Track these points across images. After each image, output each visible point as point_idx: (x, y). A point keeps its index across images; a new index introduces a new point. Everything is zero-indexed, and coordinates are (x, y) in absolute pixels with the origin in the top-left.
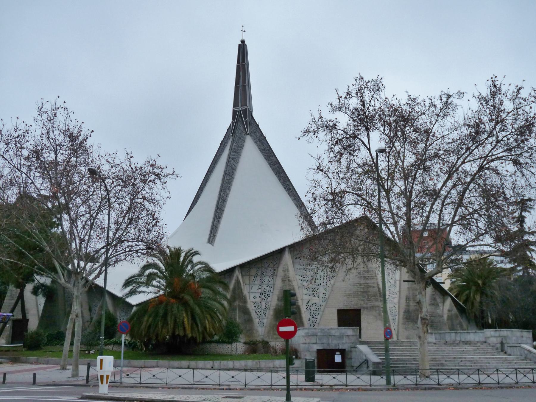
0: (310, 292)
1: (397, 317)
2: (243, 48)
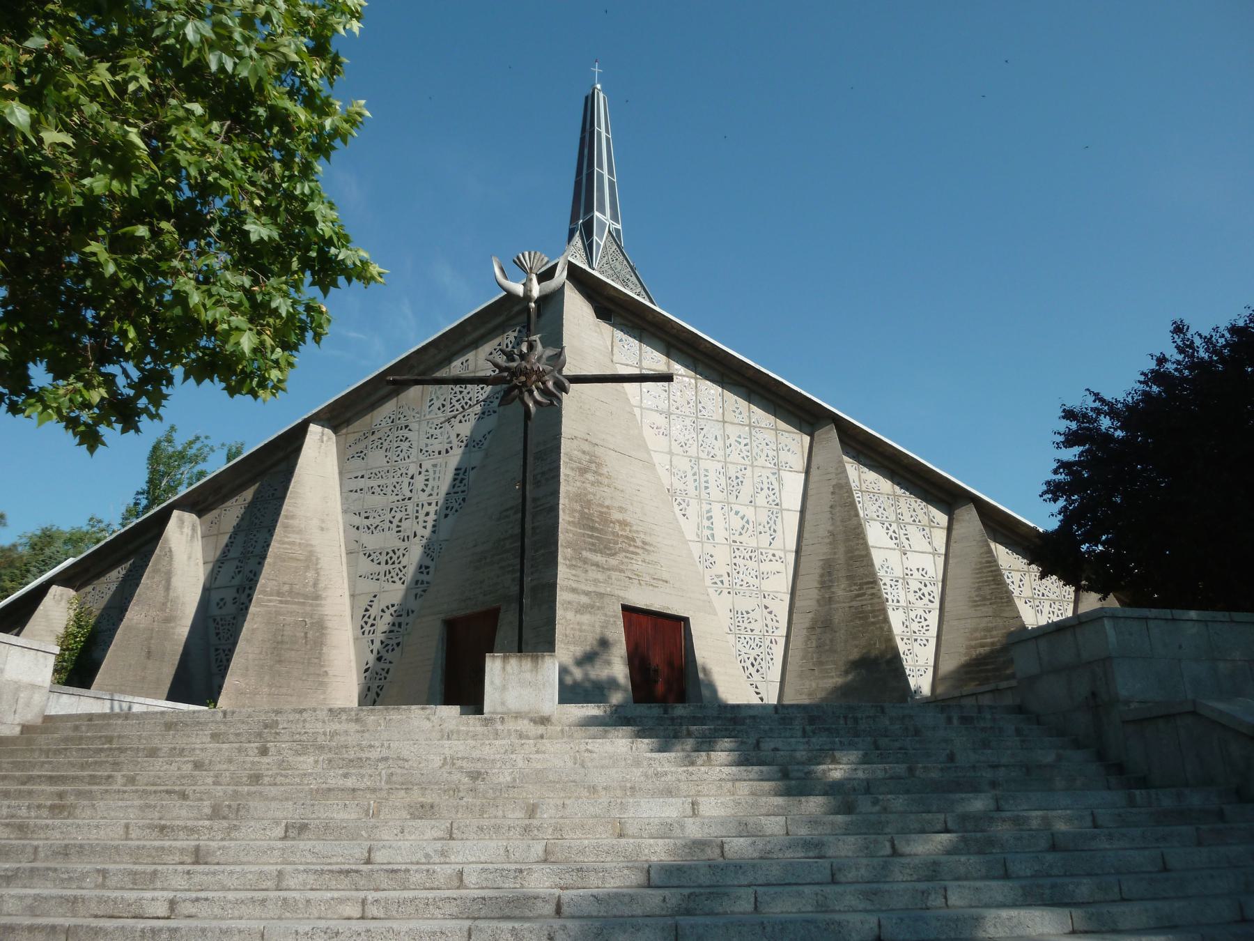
0: (377, 568)
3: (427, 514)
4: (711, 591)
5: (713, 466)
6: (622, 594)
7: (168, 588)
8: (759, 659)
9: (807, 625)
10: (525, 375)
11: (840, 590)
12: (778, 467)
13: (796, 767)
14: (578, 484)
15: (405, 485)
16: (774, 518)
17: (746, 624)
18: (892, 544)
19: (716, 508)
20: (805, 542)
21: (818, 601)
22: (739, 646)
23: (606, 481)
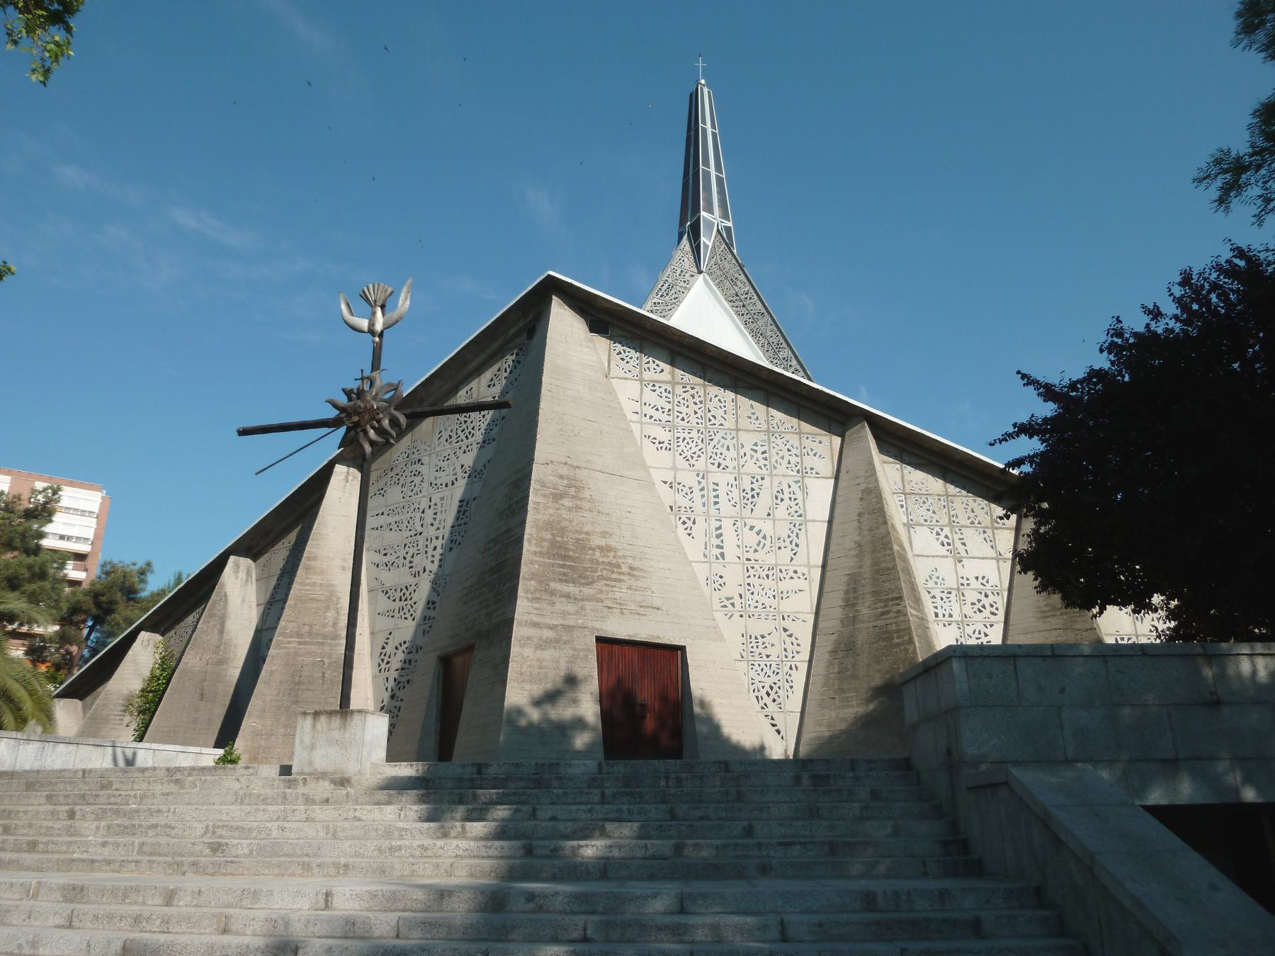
1: (799, 679)
3: (435, 548)
4: (719, 616)
5: (724, 478)
6: (597, 625)
7: (222, 632)
8: (776, 688)
9: (830, 648)
10: (358, 414)
11: (865, 610)
12: (803, 472)
13: (541, 843)
14: (551, 511)
15: (417, 520)
16: (796, 530)
17: (760, 650)
18: (943, 551)
19: (727, 525)
20: (831, 555)
21: (842, 621)
22: (752, 674)
23: (586, 505)
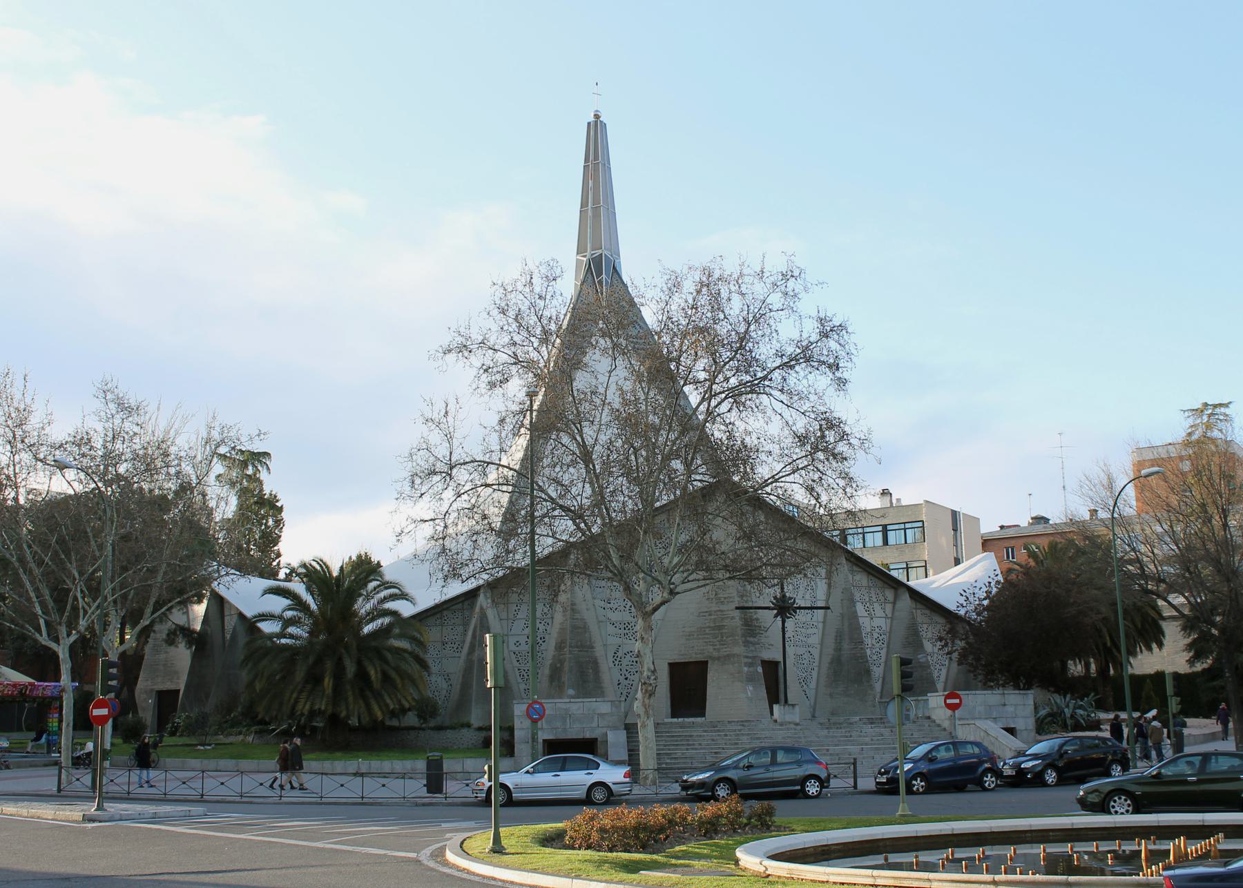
1: (815, 674)
2: (596, 131)
11: (846, 646)
